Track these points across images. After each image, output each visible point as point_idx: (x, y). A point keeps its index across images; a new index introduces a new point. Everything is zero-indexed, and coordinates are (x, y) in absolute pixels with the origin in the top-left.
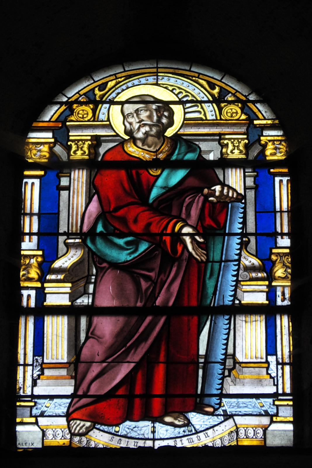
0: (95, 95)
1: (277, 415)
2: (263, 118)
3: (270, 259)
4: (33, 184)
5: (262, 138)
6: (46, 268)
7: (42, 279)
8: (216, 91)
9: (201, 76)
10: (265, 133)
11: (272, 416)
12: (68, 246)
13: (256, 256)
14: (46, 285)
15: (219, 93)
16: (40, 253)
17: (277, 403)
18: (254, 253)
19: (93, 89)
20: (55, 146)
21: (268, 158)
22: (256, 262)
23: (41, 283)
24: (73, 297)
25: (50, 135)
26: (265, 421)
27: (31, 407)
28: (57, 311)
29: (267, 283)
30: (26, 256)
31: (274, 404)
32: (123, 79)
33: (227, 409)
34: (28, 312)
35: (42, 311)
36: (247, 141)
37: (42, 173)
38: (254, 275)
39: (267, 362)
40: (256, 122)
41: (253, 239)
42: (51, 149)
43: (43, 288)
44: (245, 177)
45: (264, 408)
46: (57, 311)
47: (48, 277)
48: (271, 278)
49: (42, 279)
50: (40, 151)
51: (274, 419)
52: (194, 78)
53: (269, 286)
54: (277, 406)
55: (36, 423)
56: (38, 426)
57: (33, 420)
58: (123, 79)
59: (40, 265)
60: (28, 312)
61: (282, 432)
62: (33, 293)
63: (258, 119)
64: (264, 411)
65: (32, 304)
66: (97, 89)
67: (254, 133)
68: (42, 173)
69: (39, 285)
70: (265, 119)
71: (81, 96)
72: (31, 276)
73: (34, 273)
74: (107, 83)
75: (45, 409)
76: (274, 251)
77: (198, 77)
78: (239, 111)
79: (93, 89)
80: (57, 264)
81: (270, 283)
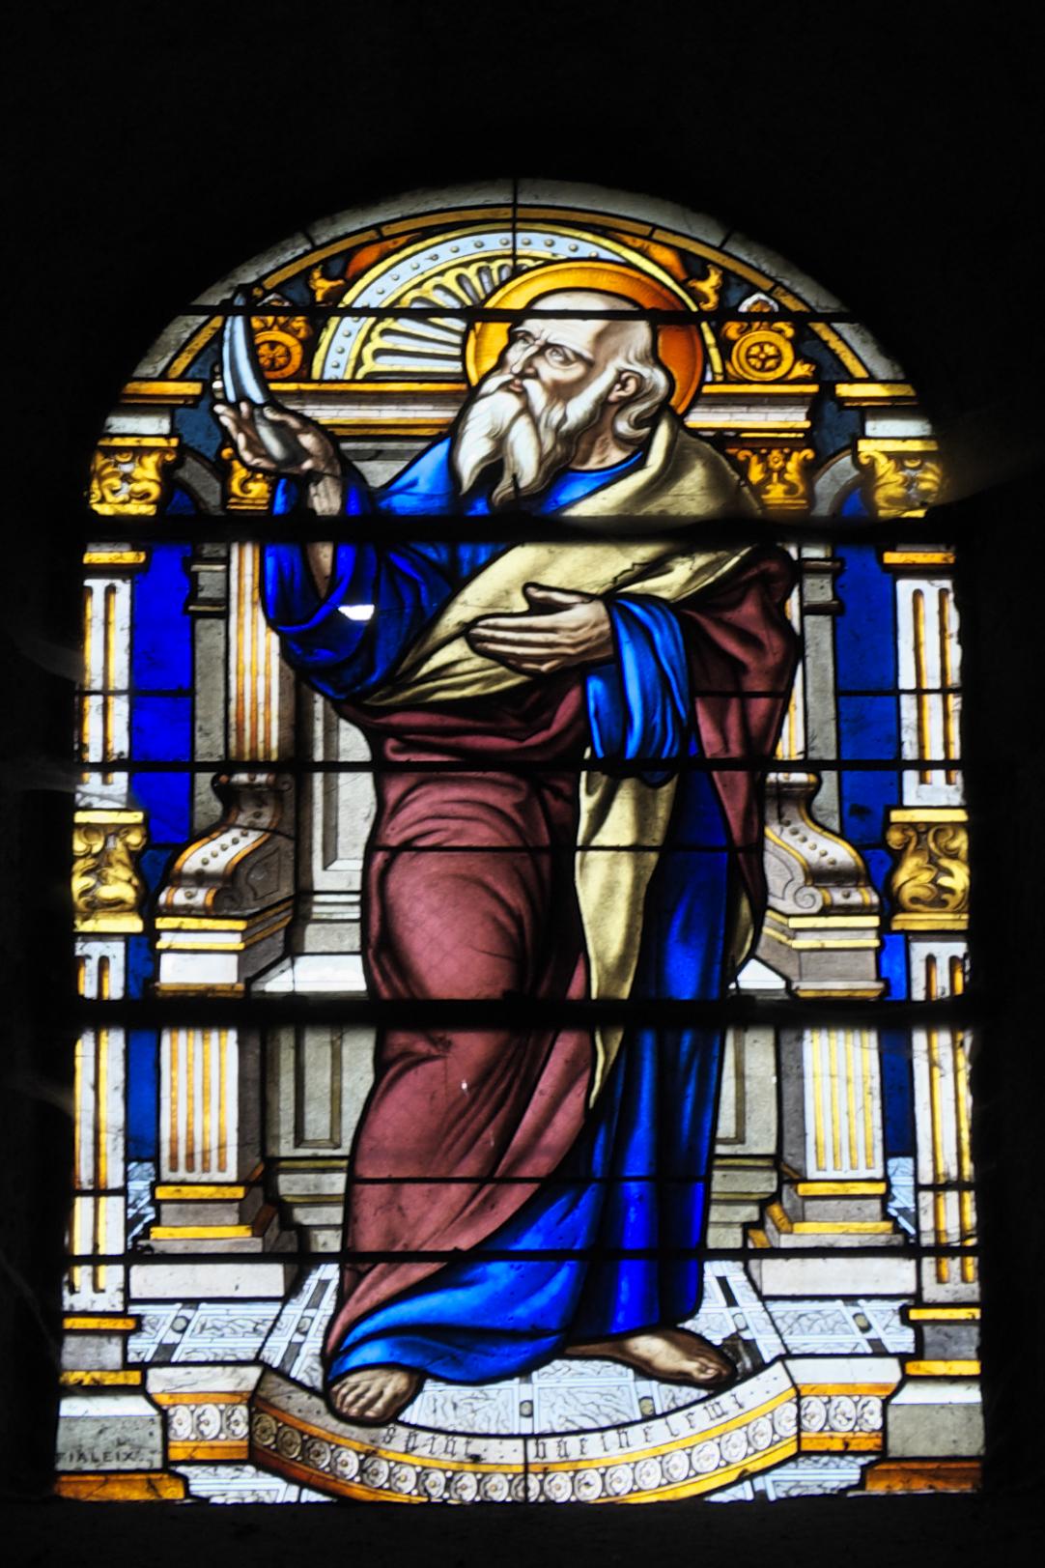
0: (313, 292)
3: (883, 843)
4: (104, 962)
6: (155, 869)
10: (872, 427)
11: (903, 1358)
12: (231, 798)
13: (842, 835)
14: (161, 923)
15: (720, 291)
16: (137, 817)
17: (914, 1315)
18: (835, 825)
19: (305, 275)
20: (179, 463)
21: (882, 513)
22: (842, 853)
23: (142, 916)
28: (201, 1010)
29: (874, 921)
30: (90, 829)
31: (905, 1320)
32: (402, 240)
33: (757, 1336)
34: (101, 1015)
35: (150, 1013)
36: (809, 453)
38: (838, 897)
39: (886, 1179)
40: (843, 390)
41: (830, 778)
42: (166, 472)
43: (151, 934)
45: (871, 1335)
46: (201, 1010)
48: (890, 905)
49: (147, 906)
50: (127, 478)
51: (913, 1368)
53: (883, 931)
54: (917, 1326)
58: (402, 240)
59: (136, 860)
60: (101, 1015)
61: (947, 1412)
62: (116, 951)
63: (852, 380)
64: (870, 1341)
65: (114, 989)
66: (316, 275)
69: (134, 924)
70: (871, 379)
71: (267, 293)
72: (106, 892)
73: (120, 885)
76: (896, 816)
77: (648, 238)
78: (788, 353)
79: (305, 275)
80: (193, 859)
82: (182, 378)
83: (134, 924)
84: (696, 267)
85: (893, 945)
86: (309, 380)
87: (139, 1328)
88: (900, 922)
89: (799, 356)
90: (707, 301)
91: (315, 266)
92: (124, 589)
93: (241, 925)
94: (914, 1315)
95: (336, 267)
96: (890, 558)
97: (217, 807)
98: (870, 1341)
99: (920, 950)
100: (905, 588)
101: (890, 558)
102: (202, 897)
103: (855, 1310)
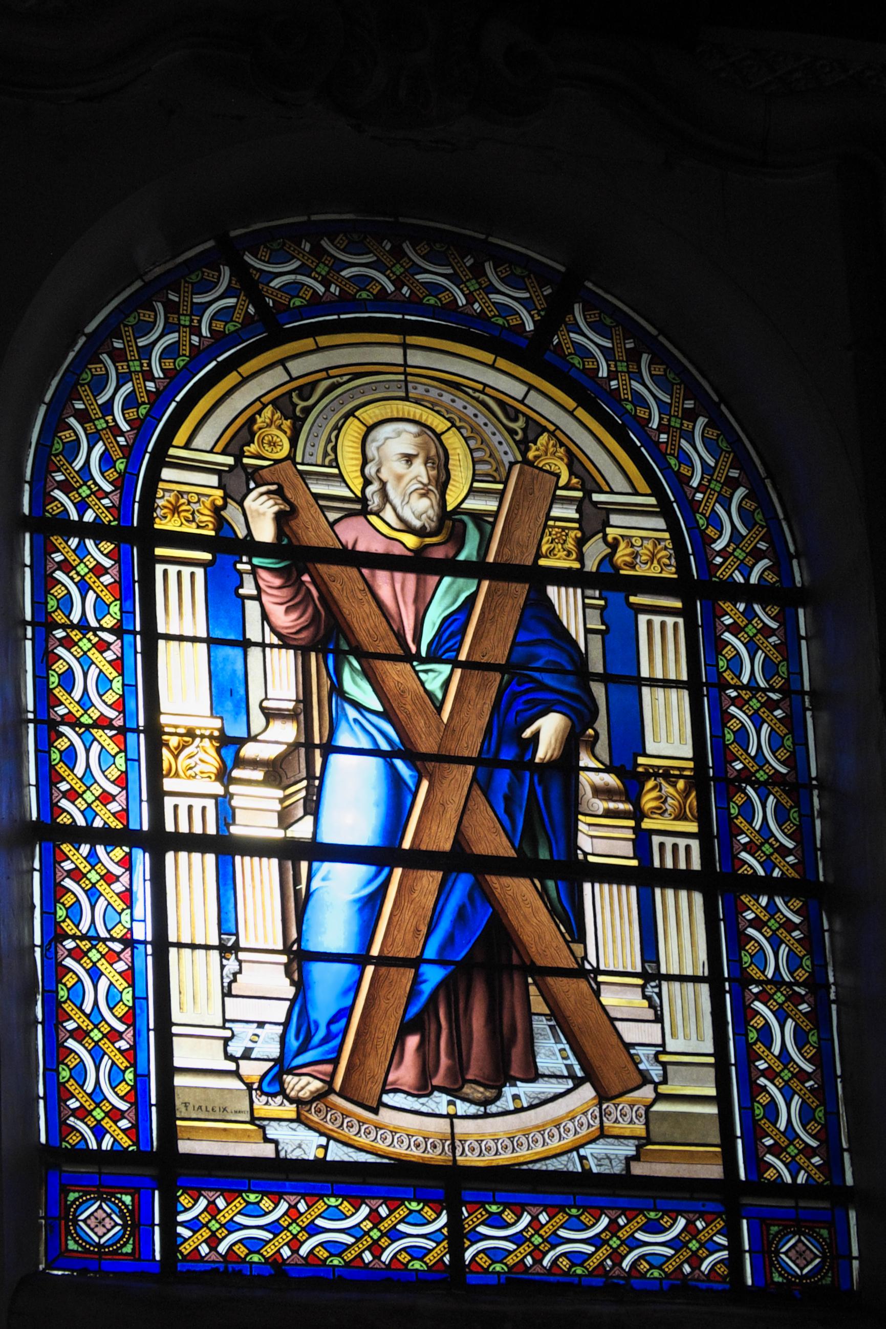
2: (608, 490)
5: (608, 530)
8: (518, 426)
9: (487, 390)
10: (615, 519)
14: (233, 789)
15: (524, 430)
19: (289, 393)
20: (224, 506)
23: (223, 784)
25: (213, 480)
37: (208, 556)
40: (596, 497)
42: (217, 511)
43: (228, 796)
44: (585, 606)
52: (477, 394)
55: (236, 1074)
56: (240, 1078)
57: (231, 1066)
63: (602, 492)
68: (208, 556)
70: (612, 492)
71: (265, 406)
74: (314, 385)
81: (638, 824)
82: (224, 453)
83: (219, 789)
84: (512, 413)
89: (572, 473)
90: (517, 434)
91: (294, 390)
92: (200, 572)
94: (664, 1058)
97: (262, 720)
100: (643, 619)
102: (259, 775)
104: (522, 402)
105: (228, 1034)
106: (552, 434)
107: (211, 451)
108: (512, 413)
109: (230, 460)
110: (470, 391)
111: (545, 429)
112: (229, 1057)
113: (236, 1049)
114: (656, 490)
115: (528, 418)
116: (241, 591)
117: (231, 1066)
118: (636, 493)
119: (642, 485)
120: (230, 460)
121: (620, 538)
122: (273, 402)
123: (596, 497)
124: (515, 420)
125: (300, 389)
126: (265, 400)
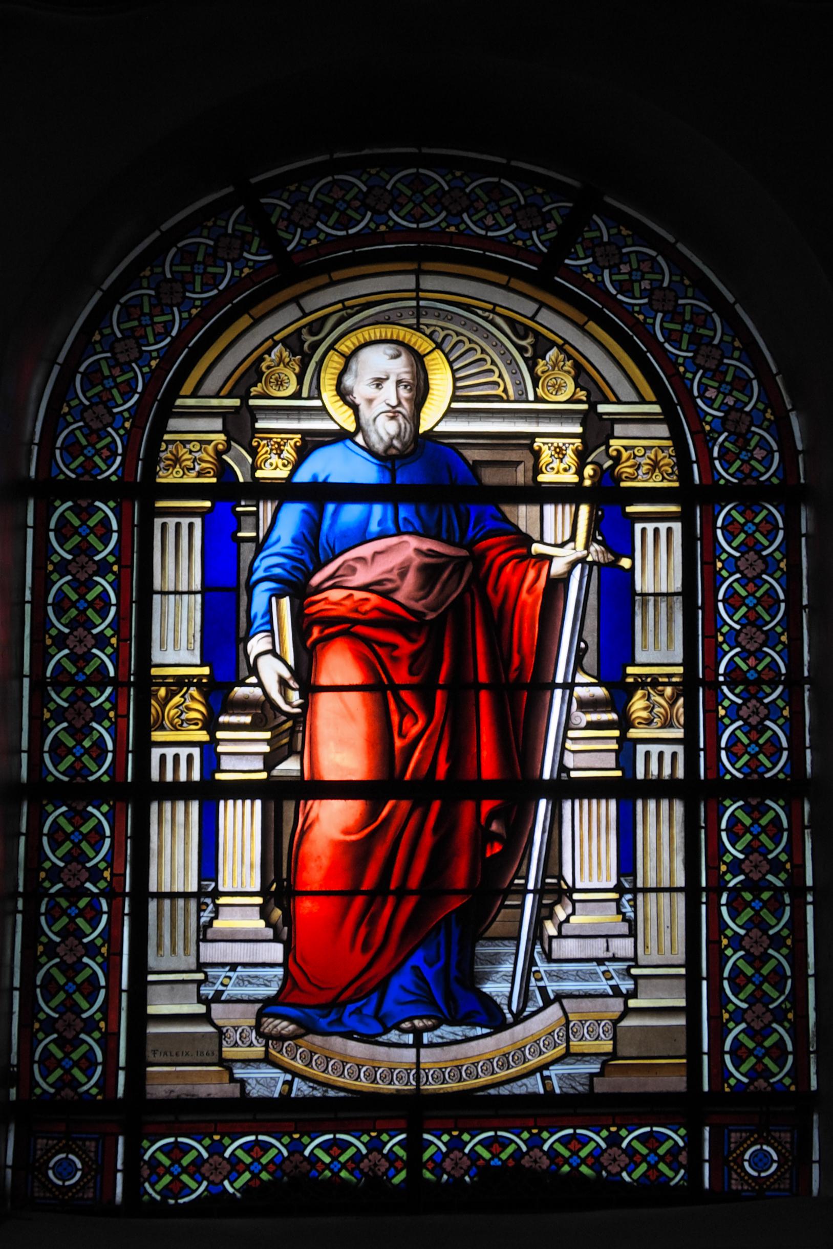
1: (633, 994)
2: (614, 400)
5: (612, 442)
7: (211, 724)
10: (619, 429)
14: (220, 735)
15: (533, 345)
17: (634, 971)
21: (623, 484)
22: (600, 692)
24: (270, 761)
26: (617, 1005)
27: (199, 983)
29: (616, 733)
38: (594, 717)
40: (602, 408)
43: (215, 742)
45: (612, 982)
47: (223, 719)
48: (625, 723)
49: (211, 724)
51: (632, 1003)
52: (487, 314)
53: (621, 740)
54: (636, 978)
57: (201, 1009)
63: (607, 401)
67: (596, 431)
69: (203, 736)
70: (619, 402)
71: (276, 344)
75: (221, 988)
77: (493, 311)
82: (229, 396)
84: (521, 331)
85: (626, 751)
86: (300, 398)
87: (206, 980)
88: (633, 733)
90: (526, 350)
91: (304, 327)
93: (267, 735)
95: (316, 327)
96: (629, 509)
98: (611, 986)
99: (641, 749)
101: (629, 509)
103: (603, 968)
104: (532, 318)
105: (200, 976)
106: (561, 349)
107: (217, 396)
108: (521, 331)
109: (236, 402)
110: (480, 312)
111: (553, 344)
112: (201, 1000)
113: (208, 991)
114: (662, 398)
115: (537, 334)
116: (240, 534)
117: (201, 1009)
118: (643, 401)
119: (649, 394)
120: (236, 402)
121: (622, 450)
122: (283, 341)
123: (602, 408)
124: (524, 338)
125: (310, 324)
126: (276, 338)
